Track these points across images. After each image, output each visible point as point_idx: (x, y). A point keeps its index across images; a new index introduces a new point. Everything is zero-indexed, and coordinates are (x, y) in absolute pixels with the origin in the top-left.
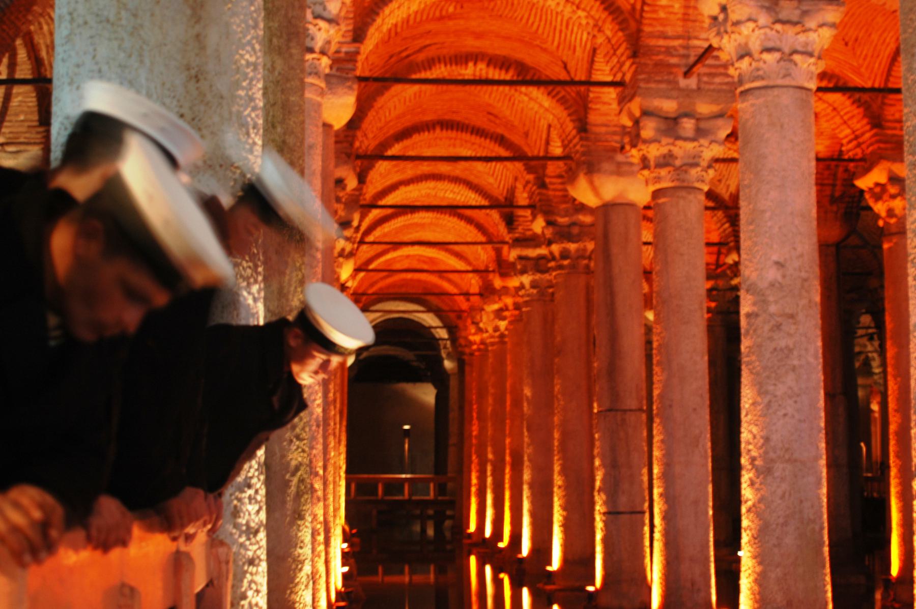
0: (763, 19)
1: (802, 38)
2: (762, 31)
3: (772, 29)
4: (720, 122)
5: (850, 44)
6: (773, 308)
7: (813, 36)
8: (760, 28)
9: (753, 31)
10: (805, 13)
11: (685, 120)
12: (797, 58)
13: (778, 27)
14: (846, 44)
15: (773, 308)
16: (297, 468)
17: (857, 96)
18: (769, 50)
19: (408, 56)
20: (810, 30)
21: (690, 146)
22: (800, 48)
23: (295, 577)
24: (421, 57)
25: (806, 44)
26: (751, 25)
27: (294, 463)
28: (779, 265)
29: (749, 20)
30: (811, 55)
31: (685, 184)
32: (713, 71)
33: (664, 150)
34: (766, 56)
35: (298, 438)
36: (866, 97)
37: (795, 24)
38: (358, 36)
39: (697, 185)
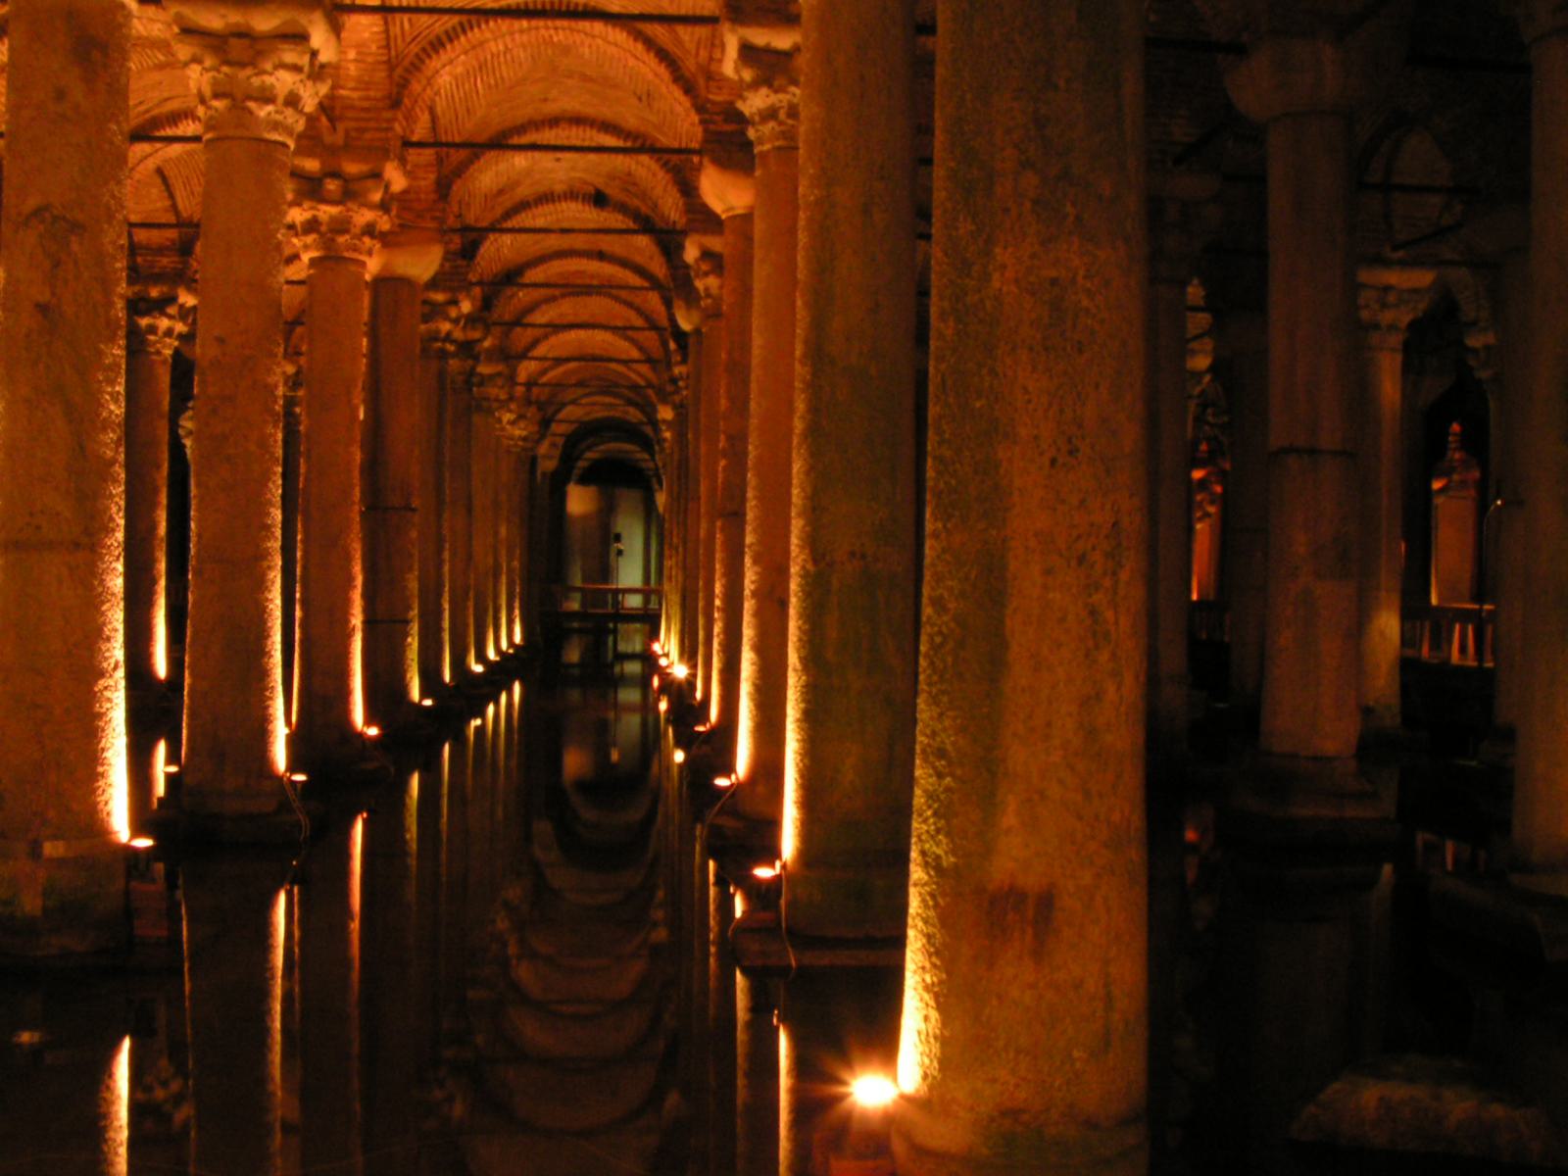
0: (208, 62)
1: (256, 81)
2: (211, 74)
3: (219, 71)
4: (370, 183)
5: (644, 98)
7: (269, 80)
8: (206, 70)
9: (201, 74)
10: (260, 53)
11: (328, 180)
12: (251, 105)
13: (225, 69)
14: (640, 99)
17: (666, 157)
18: (216, 96)
19: (147, 111)
20: (265, 72)
22: (255, 95)
25: (263, 88)
28: (220, 340)
29: (196, 60)
31: (333, 254)
32: (363, 124)
33: (308, 215)
34: (216, 104)
36: (675, 159)
37: (255, 67)
39: (346, 254)
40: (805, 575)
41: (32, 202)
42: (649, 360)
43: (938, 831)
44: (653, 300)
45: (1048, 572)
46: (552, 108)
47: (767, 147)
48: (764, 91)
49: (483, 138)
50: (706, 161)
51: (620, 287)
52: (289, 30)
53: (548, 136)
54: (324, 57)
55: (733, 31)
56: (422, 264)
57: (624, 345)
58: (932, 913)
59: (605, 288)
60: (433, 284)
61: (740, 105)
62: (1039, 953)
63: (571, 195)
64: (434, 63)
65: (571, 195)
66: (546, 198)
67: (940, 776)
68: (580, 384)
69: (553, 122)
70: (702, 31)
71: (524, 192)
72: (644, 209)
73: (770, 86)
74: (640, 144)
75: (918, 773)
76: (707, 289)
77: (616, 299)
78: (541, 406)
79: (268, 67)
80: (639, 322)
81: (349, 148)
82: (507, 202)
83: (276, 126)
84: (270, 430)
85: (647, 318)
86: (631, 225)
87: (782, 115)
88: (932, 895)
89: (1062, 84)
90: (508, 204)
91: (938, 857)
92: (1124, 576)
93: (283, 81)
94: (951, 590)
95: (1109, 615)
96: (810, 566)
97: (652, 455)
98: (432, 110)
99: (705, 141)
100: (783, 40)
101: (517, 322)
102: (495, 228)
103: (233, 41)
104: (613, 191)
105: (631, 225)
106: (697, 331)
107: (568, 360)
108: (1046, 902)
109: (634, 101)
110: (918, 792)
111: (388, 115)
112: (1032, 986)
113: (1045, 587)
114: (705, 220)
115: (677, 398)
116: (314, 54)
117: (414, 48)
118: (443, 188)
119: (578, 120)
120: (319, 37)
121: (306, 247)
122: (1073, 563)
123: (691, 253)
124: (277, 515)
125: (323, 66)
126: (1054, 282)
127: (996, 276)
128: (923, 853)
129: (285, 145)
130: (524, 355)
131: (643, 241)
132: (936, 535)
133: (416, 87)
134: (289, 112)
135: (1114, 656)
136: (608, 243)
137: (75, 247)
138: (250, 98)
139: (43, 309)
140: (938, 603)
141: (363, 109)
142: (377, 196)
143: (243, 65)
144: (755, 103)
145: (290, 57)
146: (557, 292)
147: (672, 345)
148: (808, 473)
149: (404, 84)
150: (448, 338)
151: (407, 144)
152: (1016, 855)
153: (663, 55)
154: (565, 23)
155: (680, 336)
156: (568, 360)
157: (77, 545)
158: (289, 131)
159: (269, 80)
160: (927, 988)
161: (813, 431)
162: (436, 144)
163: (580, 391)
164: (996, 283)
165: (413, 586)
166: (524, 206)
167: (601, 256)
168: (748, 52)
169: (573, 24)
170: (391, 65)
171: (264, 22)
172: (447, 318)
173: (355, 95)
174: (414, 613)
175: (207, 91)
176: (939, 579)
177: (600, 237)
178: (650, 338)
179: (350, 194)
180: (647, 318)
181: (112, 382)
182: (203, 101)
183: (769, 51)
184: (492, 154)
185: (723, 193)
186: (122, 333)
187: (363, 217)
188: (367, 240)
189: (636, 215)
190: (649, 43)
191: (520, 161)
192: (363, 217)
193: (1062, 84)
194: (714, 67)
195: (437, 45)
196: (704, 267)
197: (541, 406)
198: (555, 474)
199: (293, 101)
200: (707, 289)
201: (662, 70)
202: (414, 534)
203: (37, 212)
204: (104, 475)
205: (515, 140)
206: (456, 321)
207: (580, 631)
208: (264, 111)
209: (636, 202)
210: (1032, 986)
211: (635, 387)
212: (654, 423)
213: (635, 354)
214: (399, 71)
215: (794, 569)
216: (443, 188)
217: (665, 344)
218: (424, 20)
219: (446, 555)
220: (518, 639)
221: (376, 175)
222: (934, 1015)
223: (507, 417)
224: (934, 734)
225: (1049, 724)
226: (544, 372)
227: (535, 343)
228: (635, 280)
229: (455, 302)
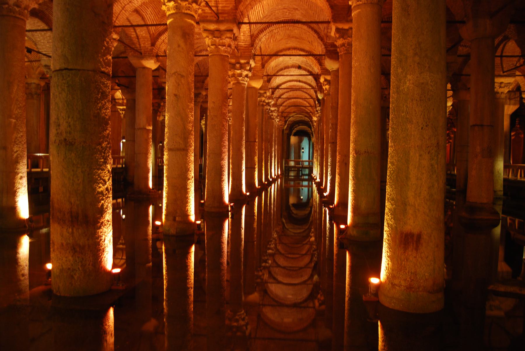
0: (210, 37)
1: (221, 41)
4: (247, 65)
6: (212, 114)
7: (224, 41)
10: (222, 35)
12: (220, 47)
13: (214, 38)
15: (212, 114)
16: (17, 151)
18: (212, 45)
21: (239, 72)
23: (15, 176)
24: (199, 49)
25: (223, 43)
26: (207, 38)
27: (15, 150)
28: (214, 102)
30: (225, 46)
33: (232, 73)
35: (17, 144)
36: (318, 57)
38: (153, 44)
40: (354, 157)
41: (173, 72)
42: (311, 106)
43: (391, 218)
44: (312, 92)
45: (420, 155)
46: (288, 45)
47: (342, 53)
48: (342, 39)
49: (272, 53)
50: (326, 57)
51: (304, 89)
52: (228, 29)
53: (288, 52)
54: (236, 35)
55: (334, 25)
56: (257, 84)
57: (305, 103)
58: (390, 238)
59: (300, 89)
60: (261, 89)
61: (335, 43)
62: (417, 249)
63: (293, 66)
64: (261, 36)
65: (293, 66)
66: (287, 67)
67: (392, 205)
68: (294, 112)
69: (289, 49)
70: (325, 25)
71: (282, 66)
72: (310, 70)
73: (343, 38)
74: (309, 54)
75: (386, 204)
76: (326, 89)
77: (303, 91)
78: (285, 118)
79: (224, 38)
80: (308, 97)
81: (242, 57)
82: (278, 69)
83: (226, 52)
84: (225, 123)
85: (310, 96)
86: (307, 73)
87: (346, 45)
88: (390, 234)
89: (425, 33)
90: (278, 69)
91: (391, 225)
92: (440, 156)
93: (227, 41)
94: (396, 160)
95: (436, 166)
96: (355, 155)
97: (311, 128)
98: (260, 47)
99: (326, 52)
100: (346, 26)
101: (279, 97)
102: (274, 75)
103: (216, 32)
104: (303, 65)
105: (307, 73)
106: (323, 99)
107: (292, 106)
108: (419, 236)
109: (308, 43)
110: (386, 209)
111: (251, 48)
112: (415, 257)
113: (419, 159)
114: (326, 72)
115: (318, 115)
116: (234, 34)
117: (256, 32)
118: (263, 66)
119: (295, 48)
120: (235, 30)
121: (232, 81)
122: (427, 153)
123: (322, 80)
124: (227, 143)
125: (236, 37)
126: (423, 83)
127: (408, 82)
128: (388, 224)
129: (228, 56)
130: (281, 105)
131: (310, 77)
132: (392, 147)
133: (257, 41)
134: (229, 48)
135: (437, 176)
136: (301, 78)
137: (183, 81)
138: (220, 45)
139: (175, 95)
140: (393, 164)
141: (245, 47)
142: (248, 68)
143: (218, 37)
144: (339, 42)
145: (229, 35)
146: (289, 90)
147: (317, 102)
148: (354, 133)
149: (254, 41)
150: (264, 101)
151: (255, 55)
152: (412, 225)
153: (316, 32)
154: (292, 25)
155: (318, 100)
156: (292, 106)
157: (184, 150)
158: (229, 53)
159: (224, 41)
160: (388, 257)
161: (356, 122)
162: (261, 55)
163: (294, 114)
164: (408, 84)
165: (256, 159)
166: (282, 69)
167: (300, 81)
168: (338, 30)
169: (294, 25)
170: (251, 36)
171: (223, 27)
172: (264, 97)
173: (243, 44)
174: (257, 166)
175: (210, 44)
176: (392, 157)
177: (300, 77)
178: (311, 101)
179: (242, 67)
180: (310, 96)
181: (191, 112)
182: (209, 46)
183: (342, 29)
184: (274, 57)
185: (331, 65)
186: (193, 101)
187: (245, 73)
188: (246, 78)
189: (308, 71)
190: (312, 29)
191: (281, 59)
192: (245, 73)
193: (425, 33)
194: (328, 34)
195: (262, 31)
196: (325, 83)
197: (285, 118)
198: (287, 134)
199: (229, 46)
200: (326, 89)
201: (315, 35)
202: (257, 148)
203: (174, 73)
204: (190, 134)
205: (280, 54)
206: (266, 97)
207: (293, 170)
208: (222, 48)
209: (308, 68)
210: (415, 257)
211: (307, 113)
212: (312, 121)
213: (308, 105)
214: (253, 38)
215: (351, 156)
216: (263, 66)
217: (315, 102)
218: (259, 25)
219: (264, 152)
220: (279, 173)
221: (248, 63)
222: (390, 263)
223: (277, 120)
224: (391, 195)
225: (420, 193)
226: (286, 109)
227: (283, 103)
228: (308, 87)
229: (266, 93)
